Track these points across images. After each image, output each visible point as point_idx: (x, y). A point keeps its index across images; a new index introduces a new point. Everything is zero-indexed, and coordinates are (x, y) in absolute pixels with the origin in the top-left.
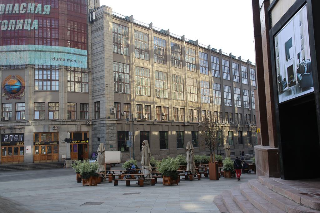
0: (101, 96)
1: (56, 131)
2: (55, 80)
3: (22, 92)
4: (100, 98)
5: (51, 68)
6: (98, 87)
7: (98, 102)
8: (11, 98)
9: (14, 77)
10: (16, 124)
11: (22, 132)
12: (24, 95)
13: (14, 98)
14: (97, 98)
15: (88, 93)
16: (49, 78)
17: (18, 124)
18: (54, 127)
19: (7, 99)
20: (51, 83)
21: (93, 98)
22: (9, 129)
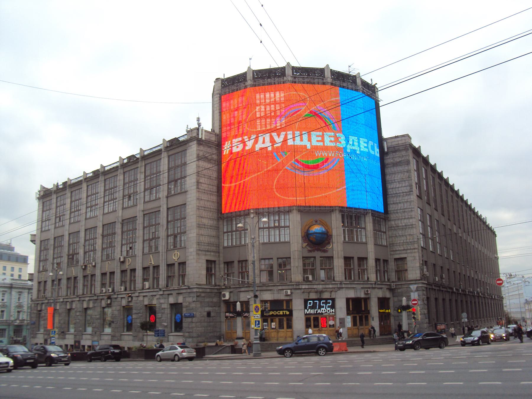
0: (409, 251)
1: (288, 298)
2: (285, 227)
3: (329, 243)
4: (406, 253)
5: (279, 211)
6: (403, 238)
7: (403, 259)
8: (314, 251)
9: (316, 222)
10: (324, 286)
11: (333, 297)
12: (333, 246)
13: (318, 250)
14: (400, 254)
15: (386, 246)
16: (277, 224)
17: (327, 286)
18: (367, 291)
19: (310, 251)
20: (279, 232)
21: (392, 253)
22: (316, 292)
